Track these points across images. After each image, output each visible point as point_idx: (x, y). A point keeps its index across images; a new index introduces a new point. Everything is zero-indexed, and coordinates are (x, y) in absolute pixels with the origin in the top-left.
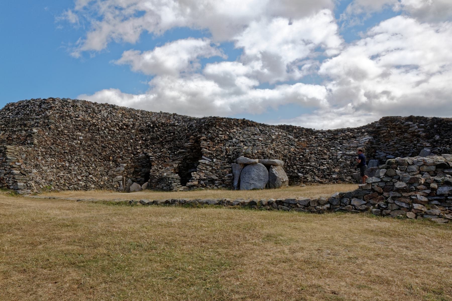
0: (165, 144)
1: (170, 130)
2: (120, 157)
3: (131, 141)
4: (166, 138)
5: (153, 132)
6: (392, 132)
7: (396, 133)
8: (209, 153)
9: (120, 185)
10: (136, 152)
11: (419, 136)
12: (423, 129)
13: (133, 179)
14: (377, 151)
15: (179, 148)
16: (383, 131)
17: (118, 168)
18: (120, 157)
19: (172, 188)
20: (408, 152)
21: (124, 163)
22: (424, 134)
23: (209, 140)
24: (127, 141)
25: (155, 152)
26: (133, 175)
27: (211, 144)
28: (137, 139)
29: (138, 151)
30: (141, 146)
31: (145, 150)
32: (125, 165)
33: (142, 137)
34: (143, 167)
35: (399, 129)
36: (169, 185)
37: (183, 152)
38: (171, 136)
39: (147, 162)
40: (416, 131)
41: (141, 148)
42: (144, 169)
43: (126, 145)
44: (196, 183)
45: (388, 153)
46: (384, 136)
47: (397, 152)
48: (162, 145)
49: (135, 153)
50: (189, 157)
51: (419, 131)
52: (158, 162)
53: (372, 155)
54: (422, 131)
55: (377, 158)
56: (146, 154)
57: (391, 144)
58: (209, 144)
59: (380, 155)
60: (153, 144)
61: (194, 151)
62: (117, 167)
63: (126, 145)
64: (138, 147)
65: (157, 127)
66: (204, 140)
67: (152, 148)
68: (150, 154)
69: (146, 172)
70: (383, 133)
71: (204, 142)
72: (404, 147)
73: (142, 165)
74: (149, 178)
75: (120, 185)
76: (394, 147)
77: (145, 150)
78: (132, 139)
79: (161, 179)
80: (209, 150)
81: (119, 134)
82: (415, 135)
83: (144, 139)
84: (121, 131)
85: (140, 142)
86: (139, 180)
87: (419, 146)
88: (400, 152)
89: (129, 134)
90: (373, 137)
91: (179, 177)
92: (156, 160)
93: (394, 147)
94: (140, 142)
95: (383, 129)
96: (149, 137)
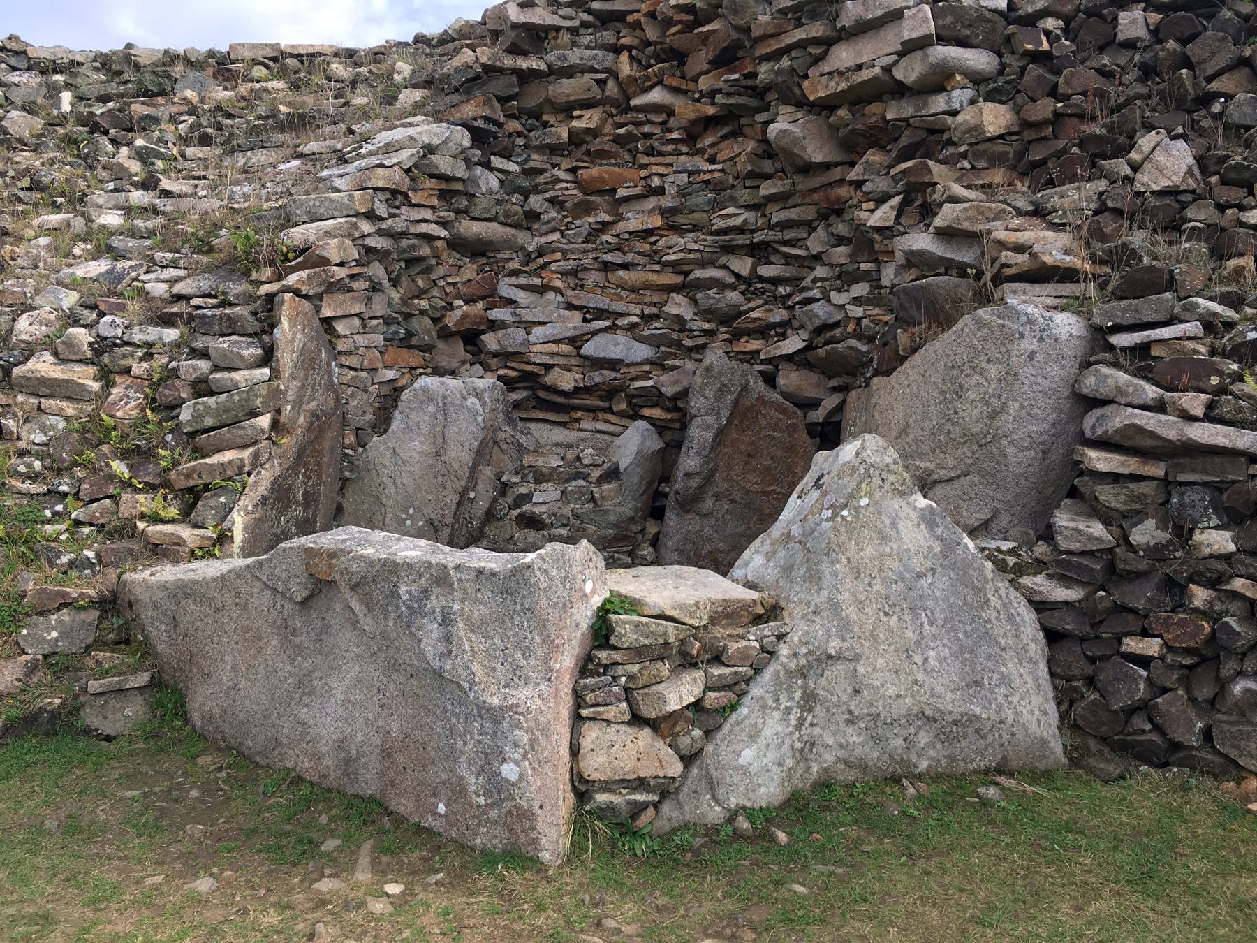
6: (656, 96)
7: (686, 110)
11: (933, 139)
12: (979, 59)
14: (506, 288)
16: (566, 88)
20: (779, 315)
22: (995, 118)
35: (725, 59)
40: (909, 72)
45: (600, 314)
46: (577, 139)
47: (679, 306)
51: (939, 81)
53: (451, 320)
54: (977, 79)
55: (505, 356)
57: (634, 221)
59: (528, 325)
70: (567, 110)
72: (743, 265)
76: (653, 256)
82: (881, 136)
87: (915, 261)
88: (707, 314)
90: (464, 138)
93: (653, 256)
95: (575, 56)
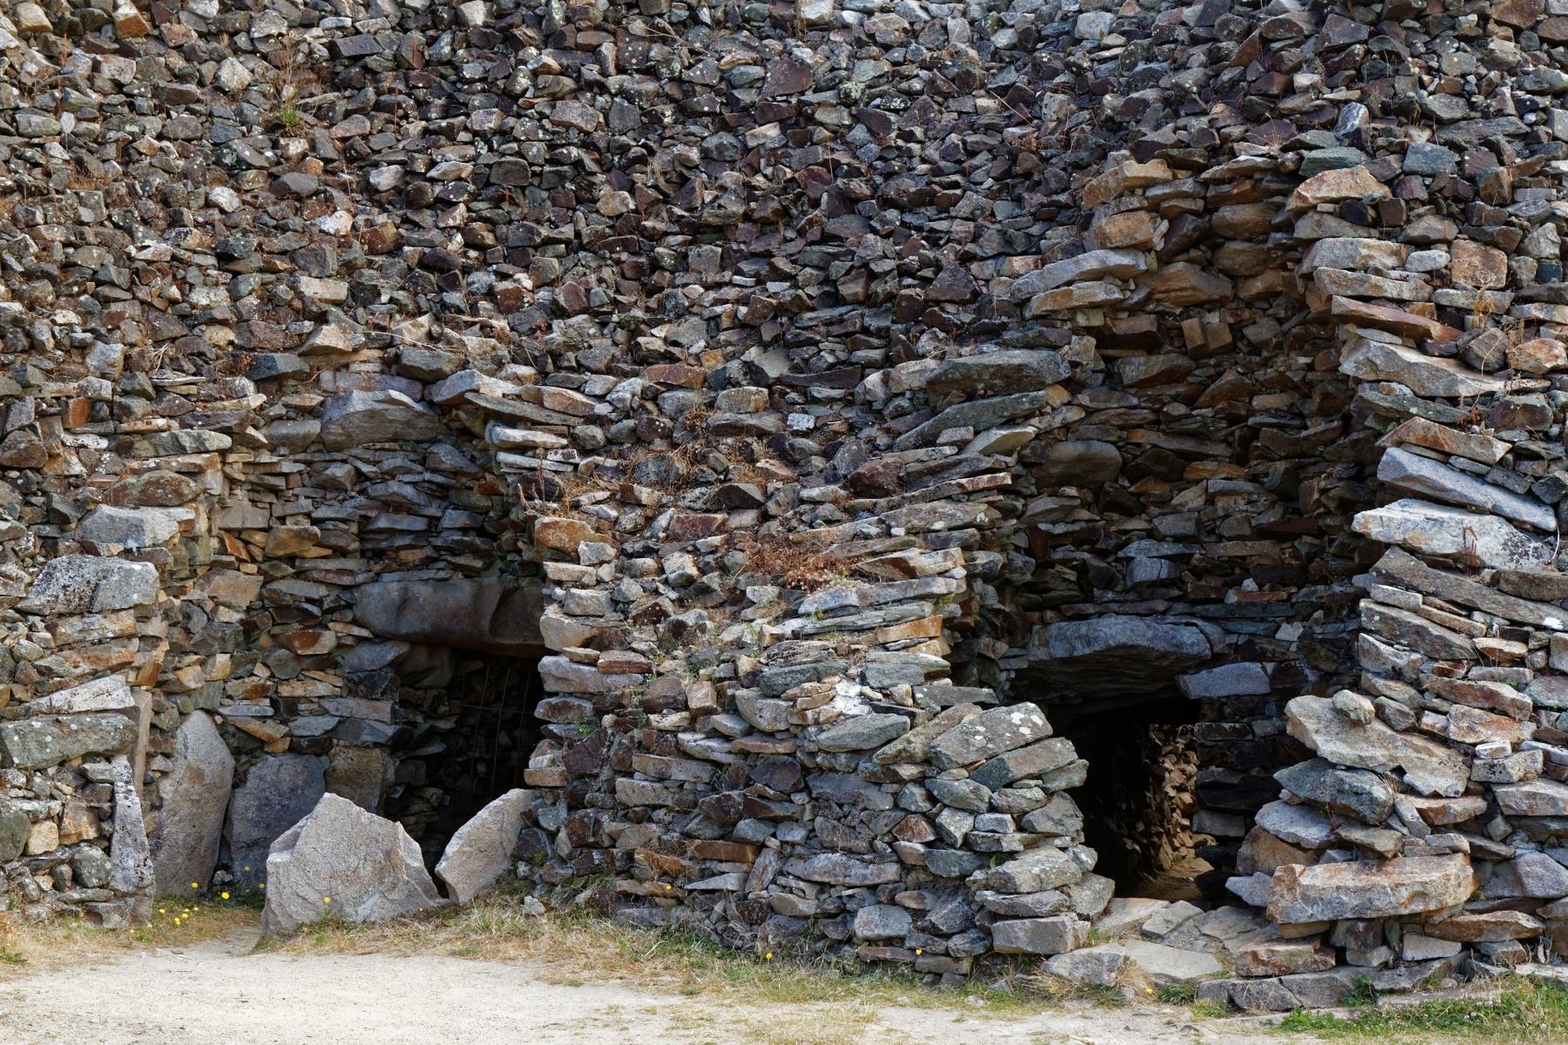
0: (682, 259)
1: (727, 82)
2: (93, 412)
3: (224, 196)
4: (680, 179)
5: (508, 100)
8: (1493, 412)
9: (104, 816)
10: (299, 345)
13: (243, 712)
15: (920, 315)
17: (70, 572)
18: (93, 412)
19: (1015, 935)
21: (147, 499)
23: (1429, 224)
24: (165, 200)
25: (550, 365)
26: (239, 671)
27: (1475, 273)
28: (293, 180)
29: (329, 336)
30: (348, 268)
31: (410, 332)
32: (161, 524)
33: (358, 158)
34: (376, 551)
36: (959, 885)
37: (1015, 379)
38: (749, 158)
39: (441, 493)
41: (362, 296)
42: (391, 586)
43: (155, 247)
44: (1447, 879)
48: (646, 276)
49: (286, 363)
50: (1069, 449)
52: (625, 499)
56: (425, 379)
58: (1438, 278)
60: (520, 256)
61: (1136, 367)
62: (50, 547)
63: (155, 247)
64: (312, 287)
65: (552, 39)
66: (1350, 211)
67: (508, 304)
68: (494, 389)
69: (411, 624)
71: (1377, 250)
73: (361, 536)
74: (535, 733)
75: (104, 816)
77: (410, 332)
78: (233, 173)
79: (774, 782)
80: (1465, 360)
81: (55, 91)
83: (385, 178)
84: (81, 63)
85: (338, 222)
86: (311, 726)
89: (183, 99)
91: (1064, 749)
92: (585, 477)
94: (338, 222)
96: (452, 160)
